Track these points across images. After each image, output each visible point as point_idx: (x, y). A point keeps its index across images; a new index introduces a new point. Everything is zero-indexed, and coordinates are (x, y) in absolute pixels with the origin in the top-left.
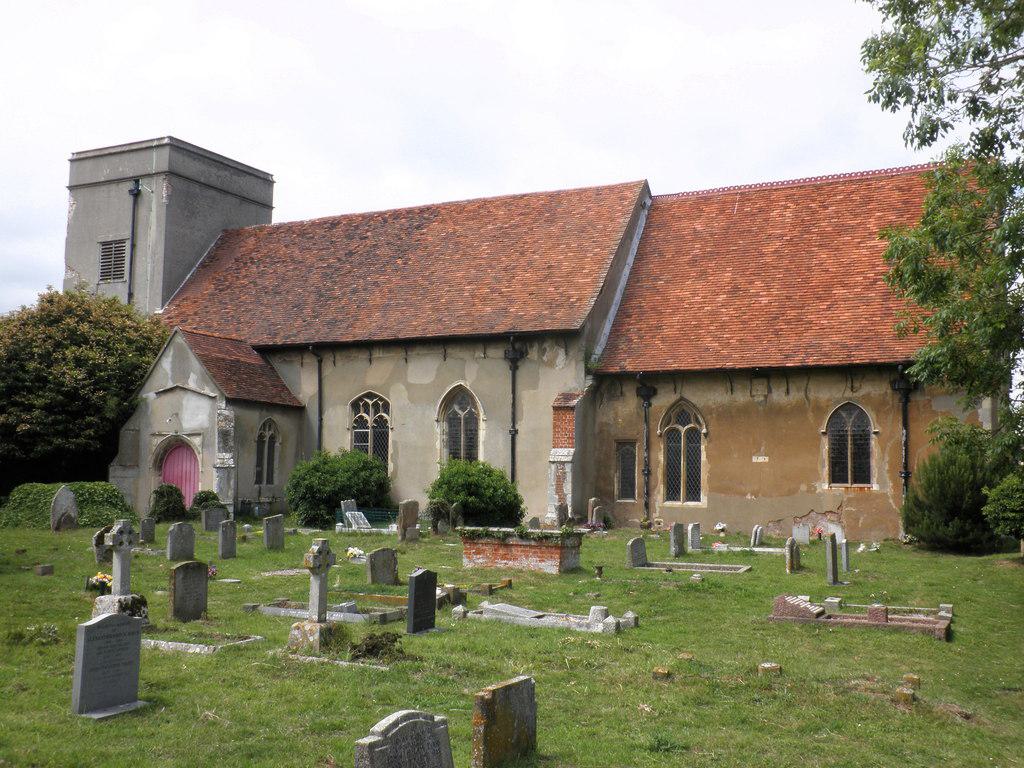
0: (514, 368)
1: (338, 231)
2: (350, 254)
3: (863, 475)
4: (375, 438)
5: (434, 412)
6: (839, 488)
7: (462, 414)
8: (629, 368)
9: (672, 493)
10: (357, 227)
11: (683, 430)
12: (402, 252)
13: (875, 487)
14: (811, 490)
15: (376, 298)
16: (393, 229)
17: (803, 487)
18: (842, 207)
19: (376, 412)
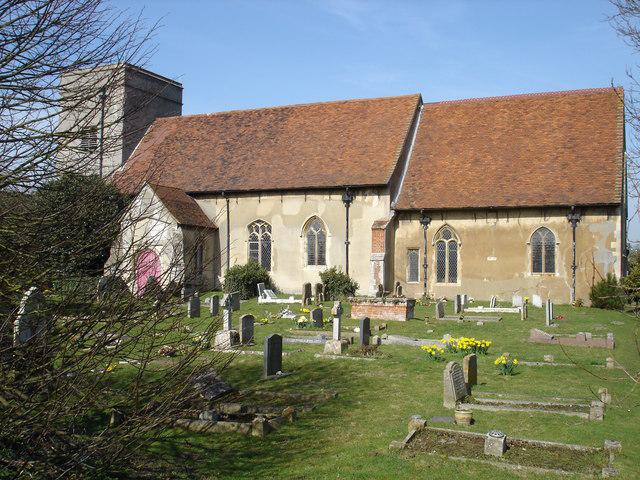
0: (348, 207)
1: (230, 121)
2: (240, 135)
3: (550, 268)
4: (262, 250)
5: (299, 230)
6: (537, 275)
7: (316, 233)
8: (416, 206)
9: (440, 277)
10: (242, 119)
11: (447, 242)
12: (272, 135)
13: (557, 274)
14: (521, 276)
15: (259, 163)
16: (266, 121)
17: (517, 275)
18: (537, 113)
19: (263, 231)
